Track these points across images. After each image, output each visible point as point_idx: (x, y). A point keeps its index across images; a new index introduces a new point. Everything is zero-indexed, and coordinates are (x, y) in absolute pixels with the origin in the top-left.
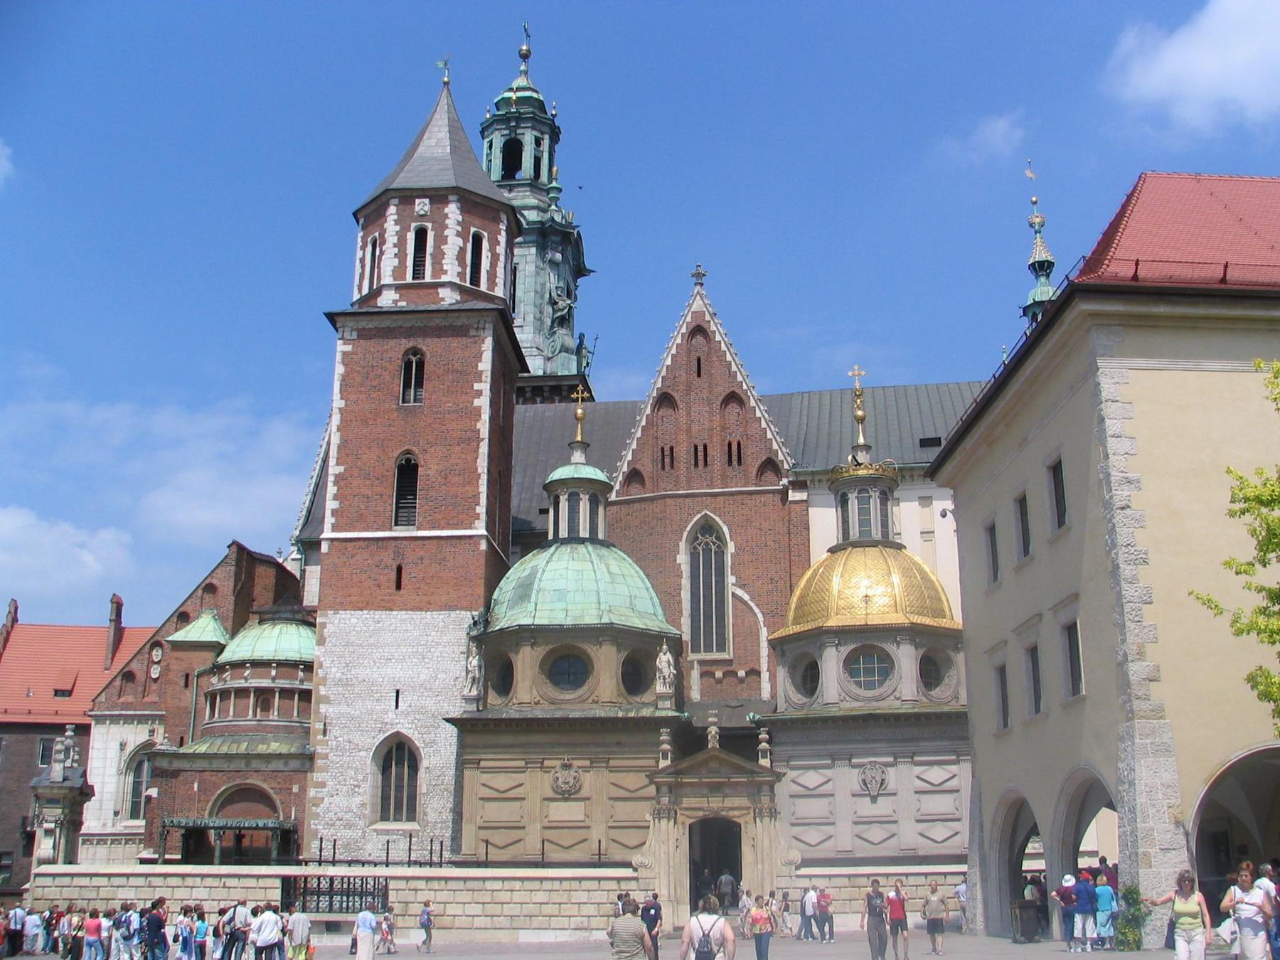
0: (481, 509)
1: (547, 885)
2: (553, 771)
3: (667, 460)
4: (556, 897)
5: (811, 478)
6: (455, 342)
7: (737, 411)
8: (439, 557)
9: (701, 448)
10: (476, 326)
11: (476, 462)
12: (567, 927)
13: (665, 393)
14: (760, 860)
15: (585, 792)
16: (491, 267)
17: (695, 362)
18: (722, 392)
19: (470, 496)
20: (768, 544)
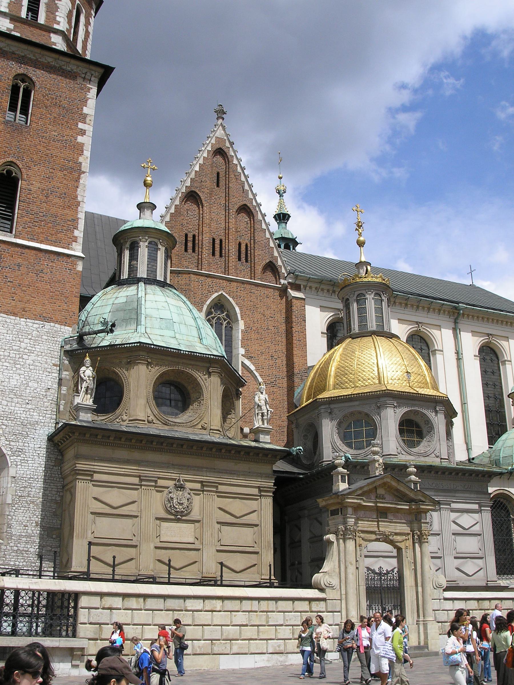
0: (79, 233)
1: (247, 605)
2: (166, 491)
3: (190, 245)
4: (255, 619)
5: (305, 283)
6: (64, 83)
7: (246, 220)
8: (36, 268)
9: (217, 242)
10: (83, 76)
11: (77, 191)
12: (265, 651)
13: (192, 191)
14: (419, 584)
15: (195, 515)
16: (85, 38)
17: (215, 175)
18: (236, 203)
19: (70, 219)
20: (270, 327)
